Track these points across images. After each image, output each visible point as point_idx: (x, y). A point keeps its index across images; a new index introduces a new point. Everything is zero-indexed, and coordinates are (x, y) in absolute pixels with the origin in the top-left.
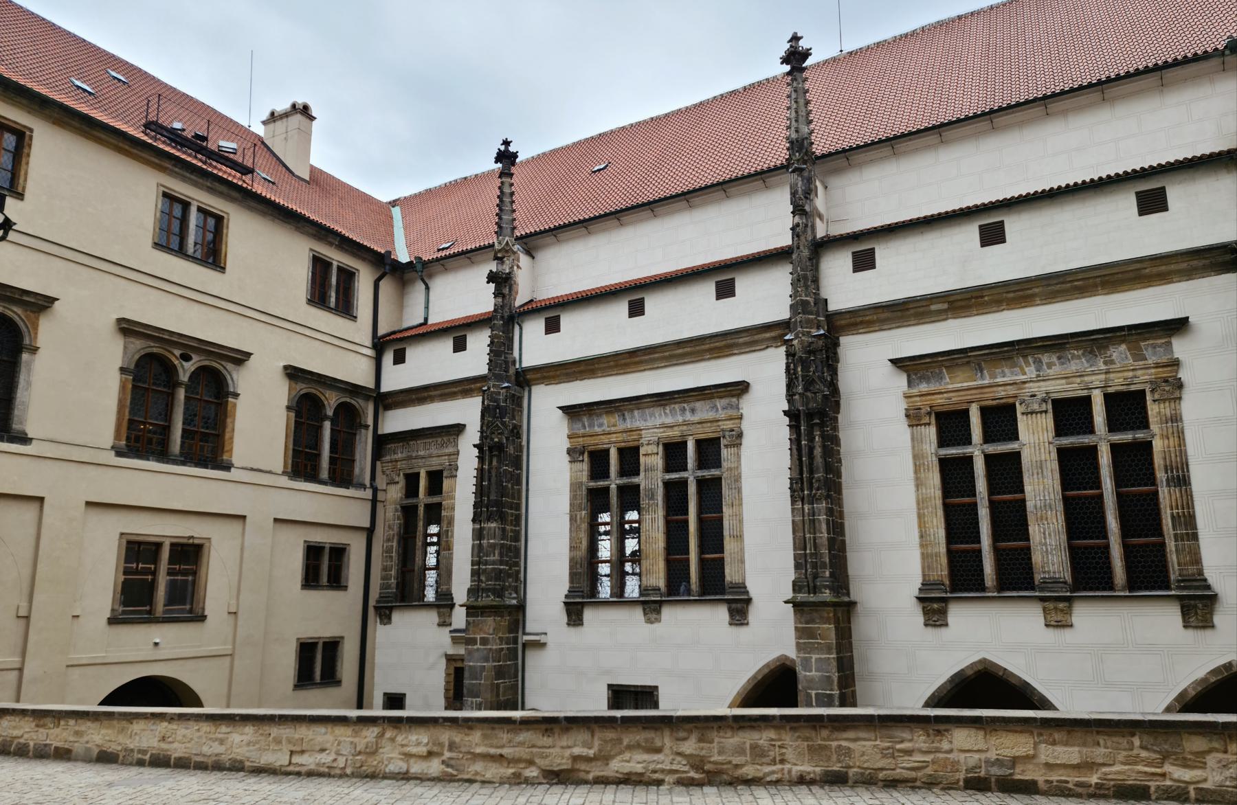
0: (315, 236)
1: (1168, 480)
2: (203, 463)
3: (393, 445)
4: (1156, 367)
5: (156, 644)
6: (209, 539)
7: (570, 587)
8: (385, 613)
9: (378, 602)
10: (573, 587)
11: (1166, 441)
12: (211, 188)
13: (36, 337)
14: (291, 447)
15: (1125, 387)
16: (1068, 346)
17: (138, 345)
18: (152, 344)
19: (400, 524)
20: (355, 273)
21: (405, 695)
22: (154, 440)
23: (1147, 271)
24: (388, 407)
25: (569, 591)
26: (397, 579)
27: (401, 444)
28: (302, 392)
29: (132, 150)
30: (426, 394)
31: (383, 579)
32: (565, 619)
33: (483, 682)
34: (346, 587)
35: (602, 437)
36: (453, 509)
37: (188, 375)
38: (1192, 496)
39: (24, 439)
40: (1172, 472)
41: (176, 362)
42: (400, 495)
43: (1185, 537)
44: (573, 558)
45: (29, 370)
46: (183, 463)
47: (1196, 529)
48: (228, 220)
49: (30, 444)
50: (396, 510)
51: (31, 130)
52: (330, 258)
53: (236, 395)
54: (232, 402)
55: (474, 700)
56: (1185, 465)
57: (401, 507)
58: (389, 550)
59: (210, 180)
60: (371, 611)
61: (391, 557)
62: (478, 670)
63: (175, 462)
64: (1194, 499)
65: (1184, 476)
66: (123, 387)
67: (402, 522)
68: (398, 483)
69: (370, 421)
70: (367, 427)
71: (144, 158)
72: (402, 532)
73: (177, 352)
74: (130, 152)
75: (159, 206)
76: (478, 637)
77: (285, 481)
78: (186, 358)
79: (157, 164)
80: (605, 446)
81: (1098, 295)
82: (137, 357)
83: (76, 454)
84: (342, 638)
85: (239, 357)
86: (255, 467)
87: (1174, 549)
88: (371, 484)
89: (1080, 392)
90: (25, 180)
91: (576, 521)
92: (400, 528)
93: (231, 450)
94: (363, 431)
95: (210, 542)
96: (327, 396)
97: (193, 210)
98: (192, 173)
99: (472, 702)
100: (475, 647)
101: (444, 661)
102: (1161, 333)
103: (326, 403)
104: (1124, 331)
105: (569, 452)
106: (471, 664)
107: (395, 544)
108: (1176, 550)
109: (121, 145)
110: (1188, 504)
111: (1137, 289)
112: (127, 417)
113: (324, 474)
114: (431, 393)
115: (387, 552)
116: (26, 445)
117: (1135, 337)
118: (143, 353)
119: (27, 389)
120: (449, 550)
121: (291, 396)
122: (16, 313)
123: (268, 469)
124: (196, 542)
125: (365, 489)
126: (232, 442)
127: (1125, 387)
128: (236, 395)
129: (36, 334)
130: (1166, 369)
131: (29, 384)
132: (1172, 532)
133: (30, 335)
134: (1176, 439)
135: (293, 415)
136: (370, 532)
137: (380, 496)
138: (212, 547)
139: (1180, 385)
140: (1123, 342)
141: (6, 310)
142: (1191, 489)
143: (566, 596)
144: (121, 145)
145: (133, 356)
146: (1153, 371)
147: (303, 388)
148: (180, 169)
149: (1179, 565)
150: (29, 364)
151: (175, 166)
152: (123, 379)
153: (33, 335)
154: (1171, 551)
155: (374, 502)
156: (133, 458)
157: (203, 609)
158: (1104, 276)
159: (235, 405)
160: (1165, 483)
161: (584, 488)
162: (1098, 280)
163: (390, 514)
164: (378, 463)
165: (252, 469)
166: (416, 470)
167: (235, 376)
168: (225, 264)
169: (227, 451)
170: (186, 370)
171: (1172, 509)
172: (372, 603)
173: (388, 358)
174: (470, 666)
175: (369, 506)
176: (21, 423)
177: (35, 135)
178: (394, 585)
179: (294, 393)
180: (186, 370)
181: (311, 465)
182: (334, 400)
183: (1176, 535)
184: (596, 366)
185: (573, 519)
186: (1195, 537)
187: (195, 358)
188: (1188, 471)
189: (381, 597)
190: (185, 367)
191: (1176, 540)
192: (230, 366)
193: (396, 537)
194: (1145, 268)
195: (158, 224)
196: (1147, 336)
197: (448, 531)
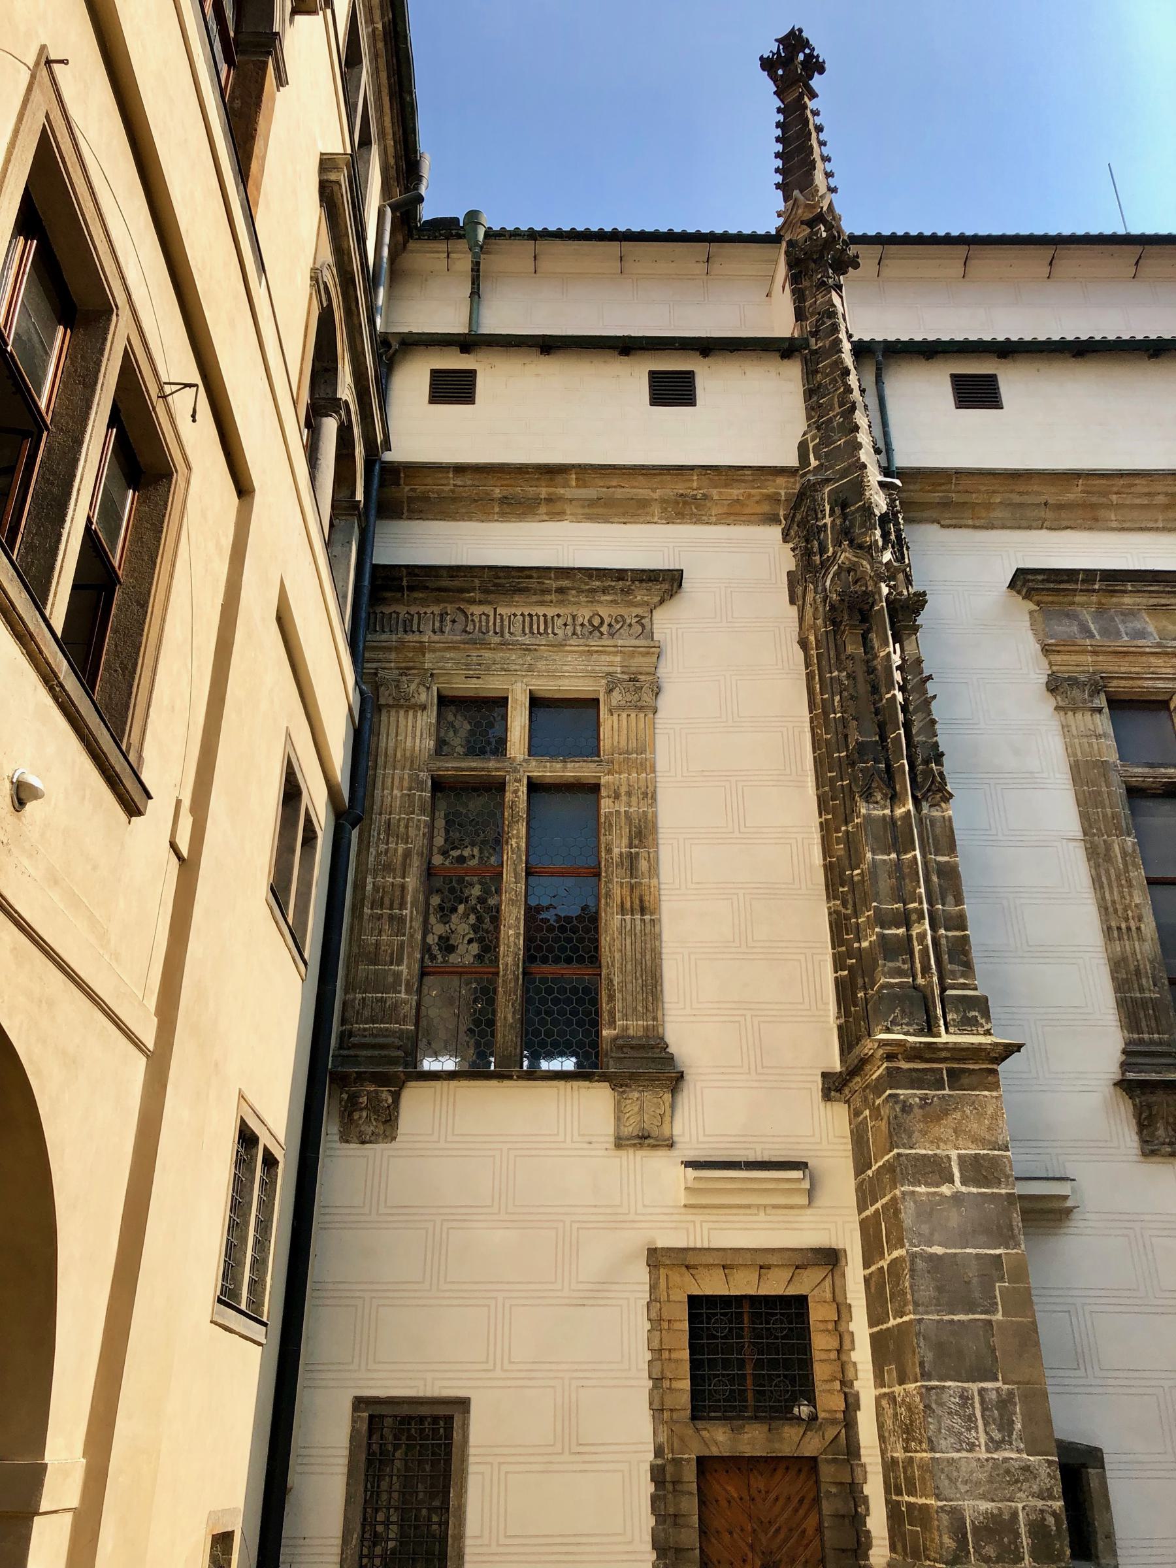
3: (402, 610)
7: (1128, 1043)
8: (374, 1098)
10: (1141, 1042)
21: (463, 1404)
25: (1124, 1052)
27: (437, 610)
30: (544, 492)
32: (1129, 1139)
33: (999, 1316)
35: (1152, 659)
36: (650, 795)
44: (1124, 959)
55: (974, 1387)
62: (972, 1273)
68: (424, 708)
76: (954, 1154)
80: (1160, 684)
91: (1108, 858)
99: (965, 1398)
100: (946, 1190)
101: (641, 1274)
105: (1054, 685)
106: (938, 1250)
114: (562, 491)
120: (643, 911)
143: (1125, 1066)
161: (1115, 779)
166: (491, 685)
174: (932, 1257)
184: (1114, 498)
185: (1097, 855)
197: (632, 859)
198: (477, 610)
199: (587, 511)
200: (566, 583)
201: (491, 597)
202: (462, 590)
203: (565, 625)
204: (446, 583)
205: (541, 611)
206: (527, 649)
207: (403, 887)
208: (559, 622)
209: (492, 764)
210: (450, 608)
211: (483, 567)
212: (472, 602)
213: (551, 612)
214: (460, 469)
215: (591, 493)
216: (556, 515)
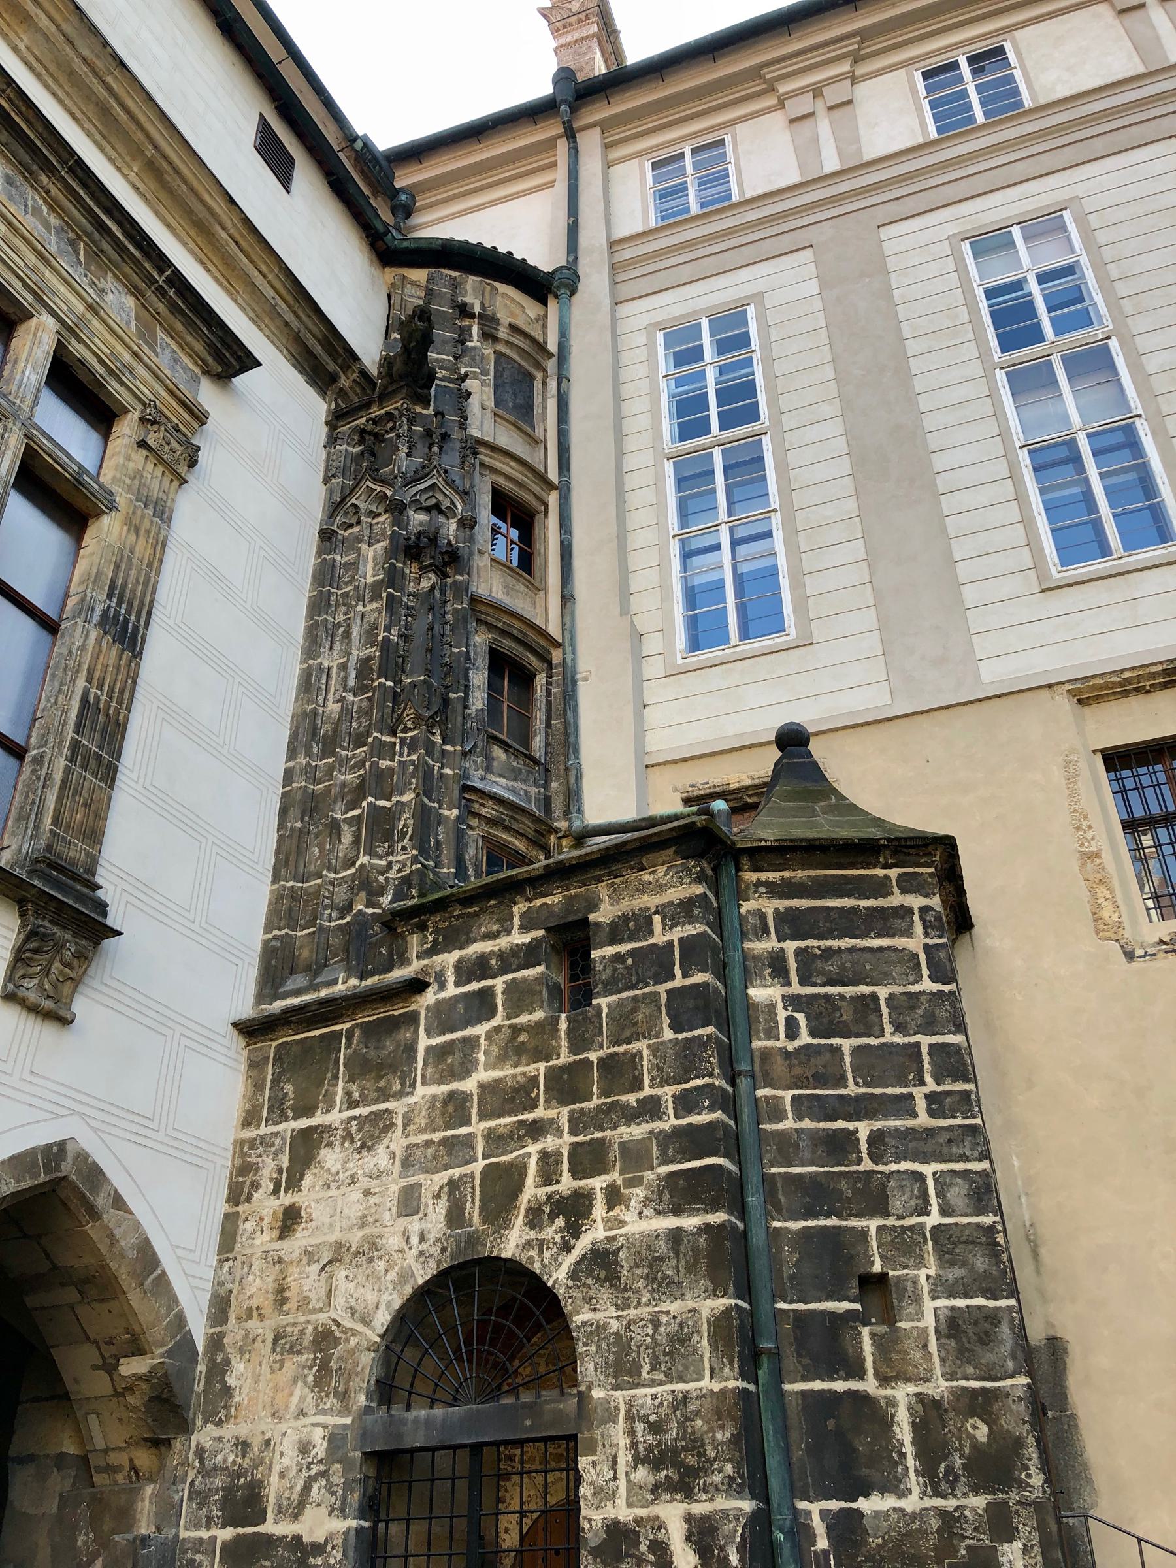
1: (105, 613)
4: (171, 392)
11: (134, 537)
15: (101, 370)
16: (44, 179)
23: (224, 235)
38: (135, 682)
40: (119, 604)
43: (92, 762)
47: (118, 759)
56: (146, 611)
64: (136, 695)
65: (136, 629)
81: (125, 176)
87: (58, 776)
89: (18, 284)
102: (199, 347)
104: (161, 272)
108: (64, 782)
110: (122, 692)
111: (185, 245)
117: (161, 307)
127: (101, 370)
130: (181, 410)
132: (70, 733)
134: (149, 550)
139: (193, 463)
140: (136, 292)
142: (138, 665)
146: (163, 393)
149: (56, 820)
154: (48, 777)
158: (165, 157)
160: (97, 617)
162: (150, 152)
171: (89, 680)
183: (75, 746)
186: (109, 774)
188: (147, 626)
191: (72, 759)
194: (224, 229)
196: (179, 327)
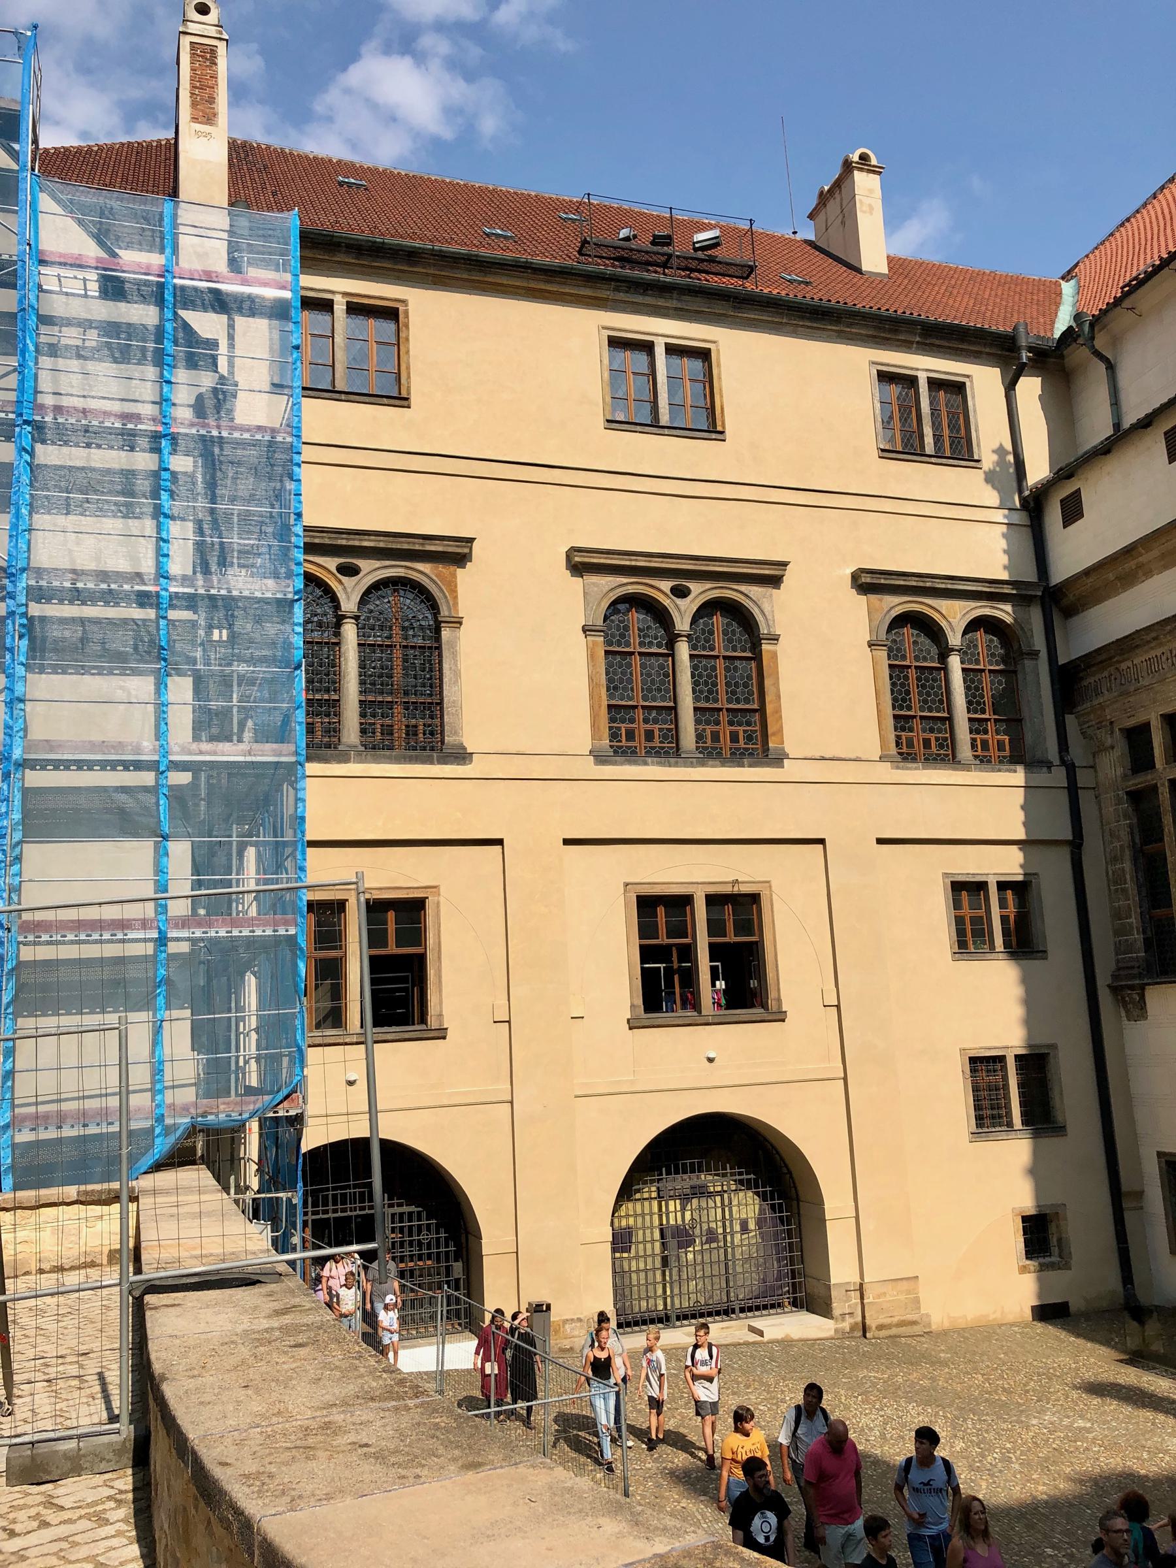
0: (875, 337)
2: (738, 757)
5: (711, 1060)
6: (768, 882)
9: (1115, 977)
12: (681, 309)
13: (456, 604)
14: (889, 712)
17: (607, 586)
18: (625, 580)
19: (1130, 826)
20: (964, 383)
22: (657, 733)
24: (1070, 612)
26: (1144, 932)
28: (894, 613)
29: (549, 287)
30: (1132, 564)
31: (1117, 933)
34: (1045, 952)
37: (688, 619)
39: (461, 756)
41: (666, 602)
42: (1120, 771)
45: (455, 655)
46: (702, 763)
48: (718, 351)
49: (471, 761)
50: (1119, 802)
51: (404, 302)
52: (912, 369)
53: (775, 639)
54: (768, 651)
57: (1128, 793)
58: (1116, 880)
59: (675, 295)
60: (1105, 997)
61: (1124, 891)
63: (689, 762)
66: (592, 656)
67: (1135, 821)
68: (1113, 747)
69: (1039, 642)
70: (1034, 654)
71: (571, 295)
72: (1137, 841)
73: (666, 585)
74: (549, 292)
75: (606, 361)
77: (886, 772)
78: (680, 592)
79: (589, 297)
82: (605, 604)
83: (536, 768)
84: (1053, 1047)
85: (767, 572)
86: (827, 756)
88: (1062, 759)
90: (409, 377)
92: (1132, 833)
93: (780, 730)
94: (1028, 663)
95: (770, 887)
96: (944, 612)
97: (660, 351)
98: (644, 294)
103: (943, 624)
107: (1127, 865)
109: (532, 285)
112: (605, 703)
113: (965, 751)
114: (1141, 559)
115: (1116, 883)
116: (464, 764)
118: (613, 596)
119: (456, 682)
121: (876, 623)
122: (423, 572)
123: (853, 756)
124: (745, 889)
125: (1049, 768)
126: (781, 717)
128: (775, 639)
129: (456, 598)
131: (457, 674)
133: (447, 602)
135: (882, 654)
136: (1076, 845)
137: (1083, 778)
138: (775, 897)
141: (410, 572)
144: (532, 285)
145: (599, 604)
147: (896, 604)
148: (627, 292)
150: (453, 644)
151: (617, 289)
152: (590, 645)
153: (451, 603)
155: (1073, 789)
156: (622, 764)
157: (779, 1000)
159: (774, 655)
163: (1109, 810)
164: (1070, 720)
165: (823, 759)
167: (766, 607)
168: (723, 425)
169: (774, 734)
170: (683, 613)
172: (1103, 980)
173: (1054, 515)
175: (1064, 797)
176: (456, 733)
177: (411, 308)
178: (1140, 944)
179: (878, 617)
180: (683, 613)
181: (937, 739)
182: (959, 616)
187: (695, 587)
189: (1119, 969)
190: (683, 608)
192: (754, 591)
193: (1128, 854)
195: (608, 389)
198: (1123, 666)
199: (1163, 563)
200: (1153, 635)
201: (1126, 656)
202: (1110, 658)
203: (1168, 659)
204: (1100, 658)
205: (1153, 654)
206: (1148, 688)
207: (1123, 870)
208: (1164, 658)
209: (1149, 777)
210: (1112, 669)
211: (1109, 644)
212: (1120, 662)
213: (1158, 652)
214: (1087, 572)
215: (1155, 553)
216: (1149, 574)
